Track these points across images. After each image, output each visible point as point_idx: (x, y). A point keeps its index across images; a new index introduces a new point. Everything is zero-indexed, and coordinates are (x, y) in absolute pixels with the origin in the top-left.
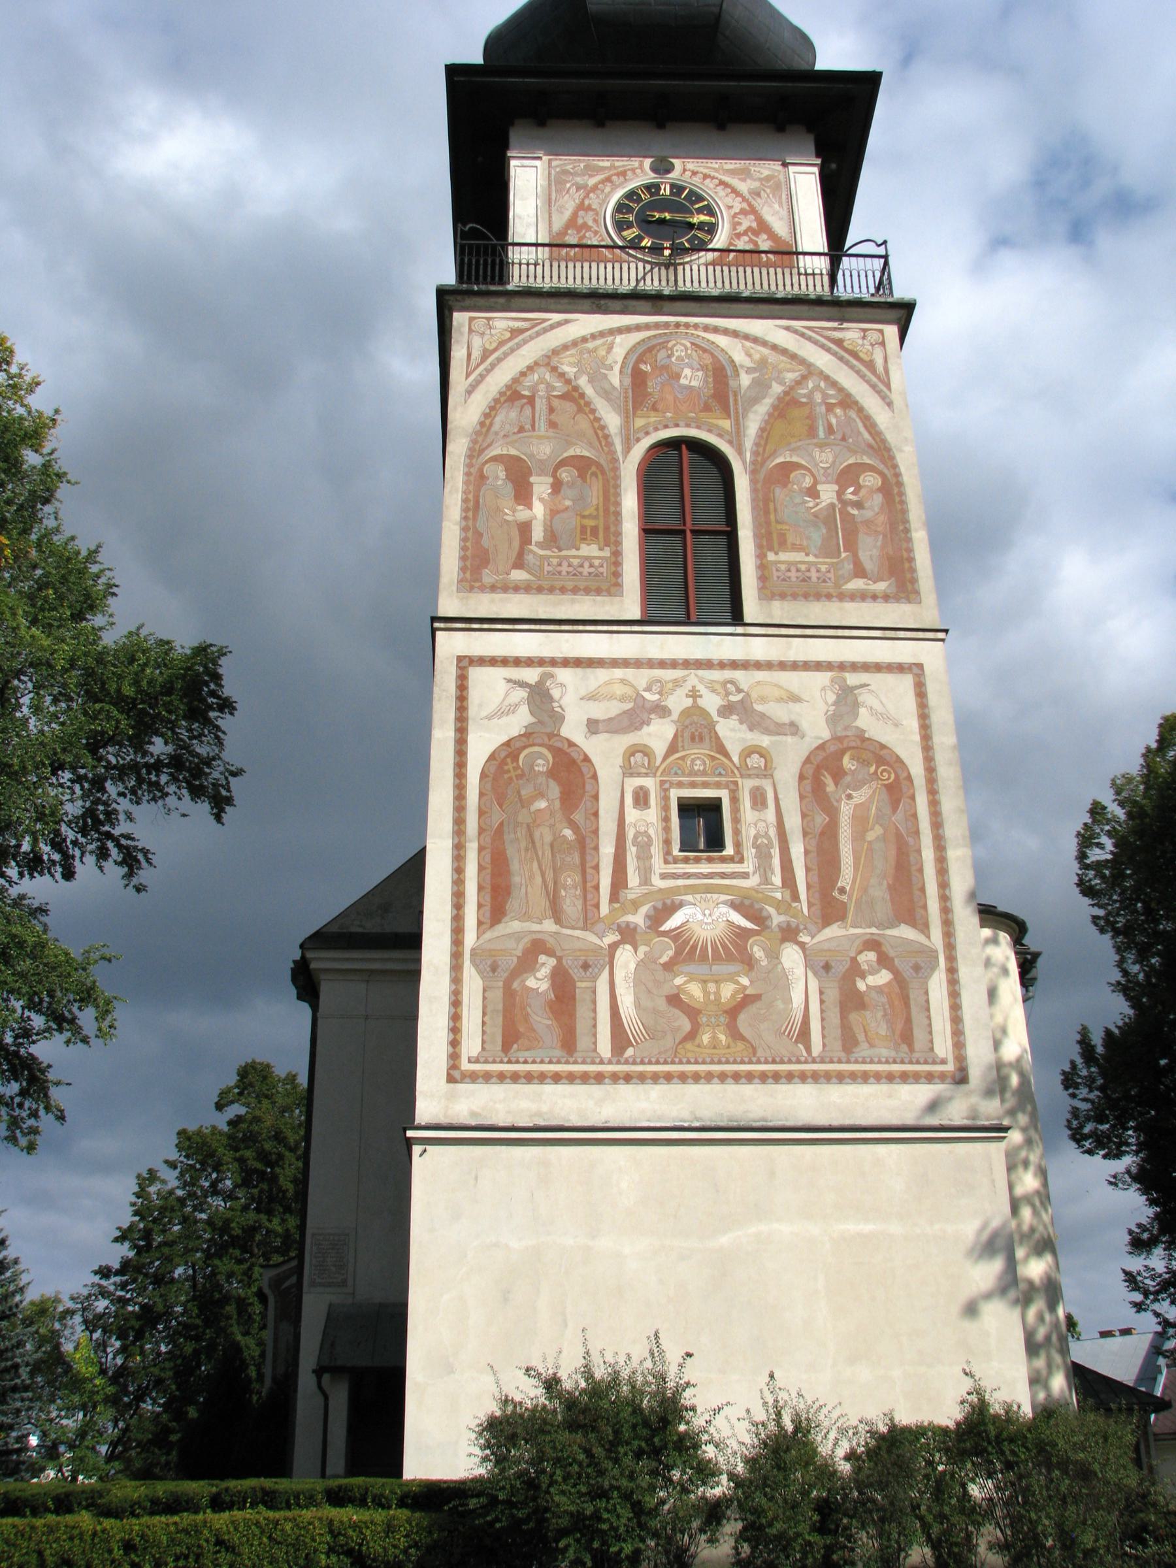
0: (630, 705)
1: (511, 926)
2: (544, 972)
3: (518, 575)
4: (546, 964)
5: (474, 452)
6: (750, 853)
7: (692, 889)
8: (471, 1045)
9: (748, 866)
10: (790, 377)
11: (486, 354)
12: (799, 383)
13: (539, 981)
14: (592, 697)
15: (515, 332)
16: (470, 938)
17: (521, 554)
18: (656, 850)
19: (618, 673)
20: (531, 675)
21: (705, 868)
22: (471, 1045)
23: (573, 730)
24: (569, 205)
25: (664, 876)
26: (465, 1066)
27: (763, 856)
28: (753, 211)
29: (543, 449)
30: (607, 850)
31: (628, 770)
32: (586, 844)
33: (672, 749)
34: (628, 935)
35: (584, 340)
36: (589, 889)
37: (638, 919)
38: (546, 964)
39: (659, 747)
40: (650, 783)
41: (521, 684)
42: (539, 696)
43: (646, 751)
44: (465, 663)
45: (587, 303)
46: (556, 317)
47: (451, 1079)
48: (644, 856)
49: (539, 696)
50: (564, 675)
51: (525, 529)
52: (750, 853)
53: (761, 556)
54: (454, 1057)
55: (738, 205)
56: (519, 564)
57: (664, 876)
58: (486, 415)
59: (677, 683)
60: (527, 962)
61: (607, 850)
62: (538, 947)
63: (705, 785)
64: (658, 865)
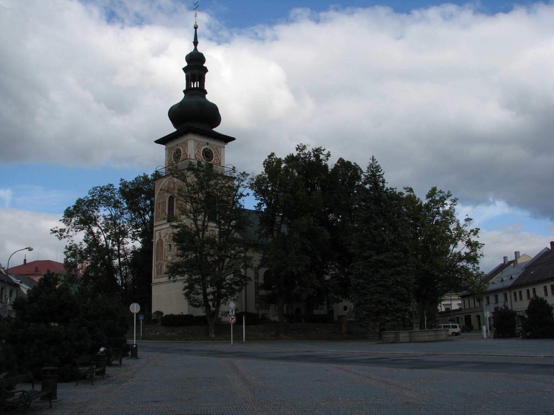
0: (165, 234)
1: (158, 262)
2: (160, 266)
3: (159, 219)
4: (160, 265)
5: (156, 202)
6: (173, 250)
7: (168, 255)
8: (155, 275)
9: (172, 252)
10: (180, 182)
11: (158, 188)
12: (180, 183)
13: (159, 267)
14: (163, 233)
15: (160, 184)
16: (155, 264)
17: (159, 216)
18: (167, 251)
19: (165, 230)
20: (159, 232)
21: (169, 253)
22: (155, 275)
23: (162, 238)
24: (170, 156)
25: (168, 254)
26: (155, 277)
27: (173, 250)
28: (184, 150)
29: (161, 201)
30: (164, 252)
31: (165, 242)
32: (162, 252)
33: (168, 238)
34: (165, 261)
35: (164, 183)
36: (163, 256)
37: (165, 259)
38: (160, 265)
39: (167, 239)
40: (166, 243)
41: (159, 233)
42: (160, 234)
43: (166, 239)
44: (156, 231)
45: (164, 178)
46: (162, 180)
47: (154, 278)
48: (166, 252)
49: (160, 234)
50: (162, 231)
51: (159, 212)
52: (173, 250)
53: (175, 211)
54: (154, 276)
55: (183, 150)
56: (159, 217)
57: (168, 254)
58: (157, 197)
59: (169, 230)
60: (159, 266)
61: (164, 252)
62: (159, 264)
63: (170, 243)
64: (167, 253)
